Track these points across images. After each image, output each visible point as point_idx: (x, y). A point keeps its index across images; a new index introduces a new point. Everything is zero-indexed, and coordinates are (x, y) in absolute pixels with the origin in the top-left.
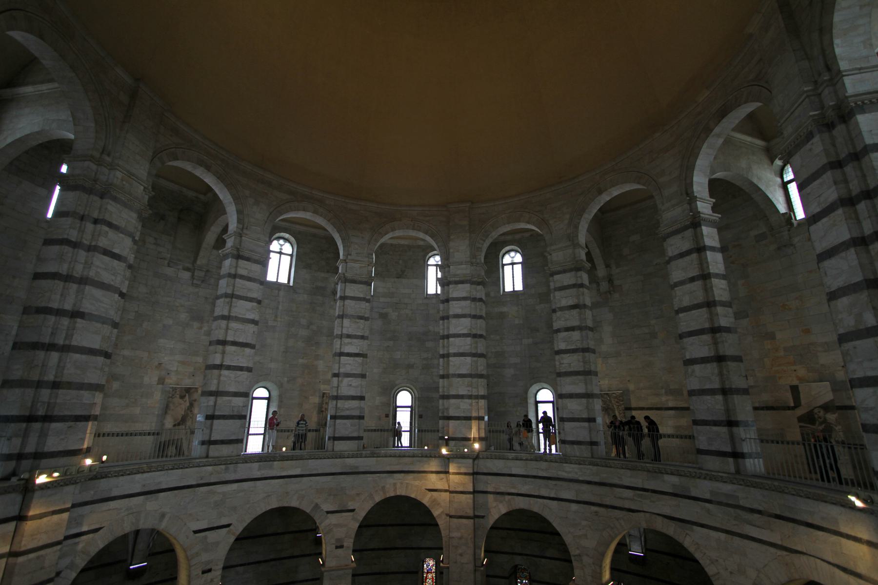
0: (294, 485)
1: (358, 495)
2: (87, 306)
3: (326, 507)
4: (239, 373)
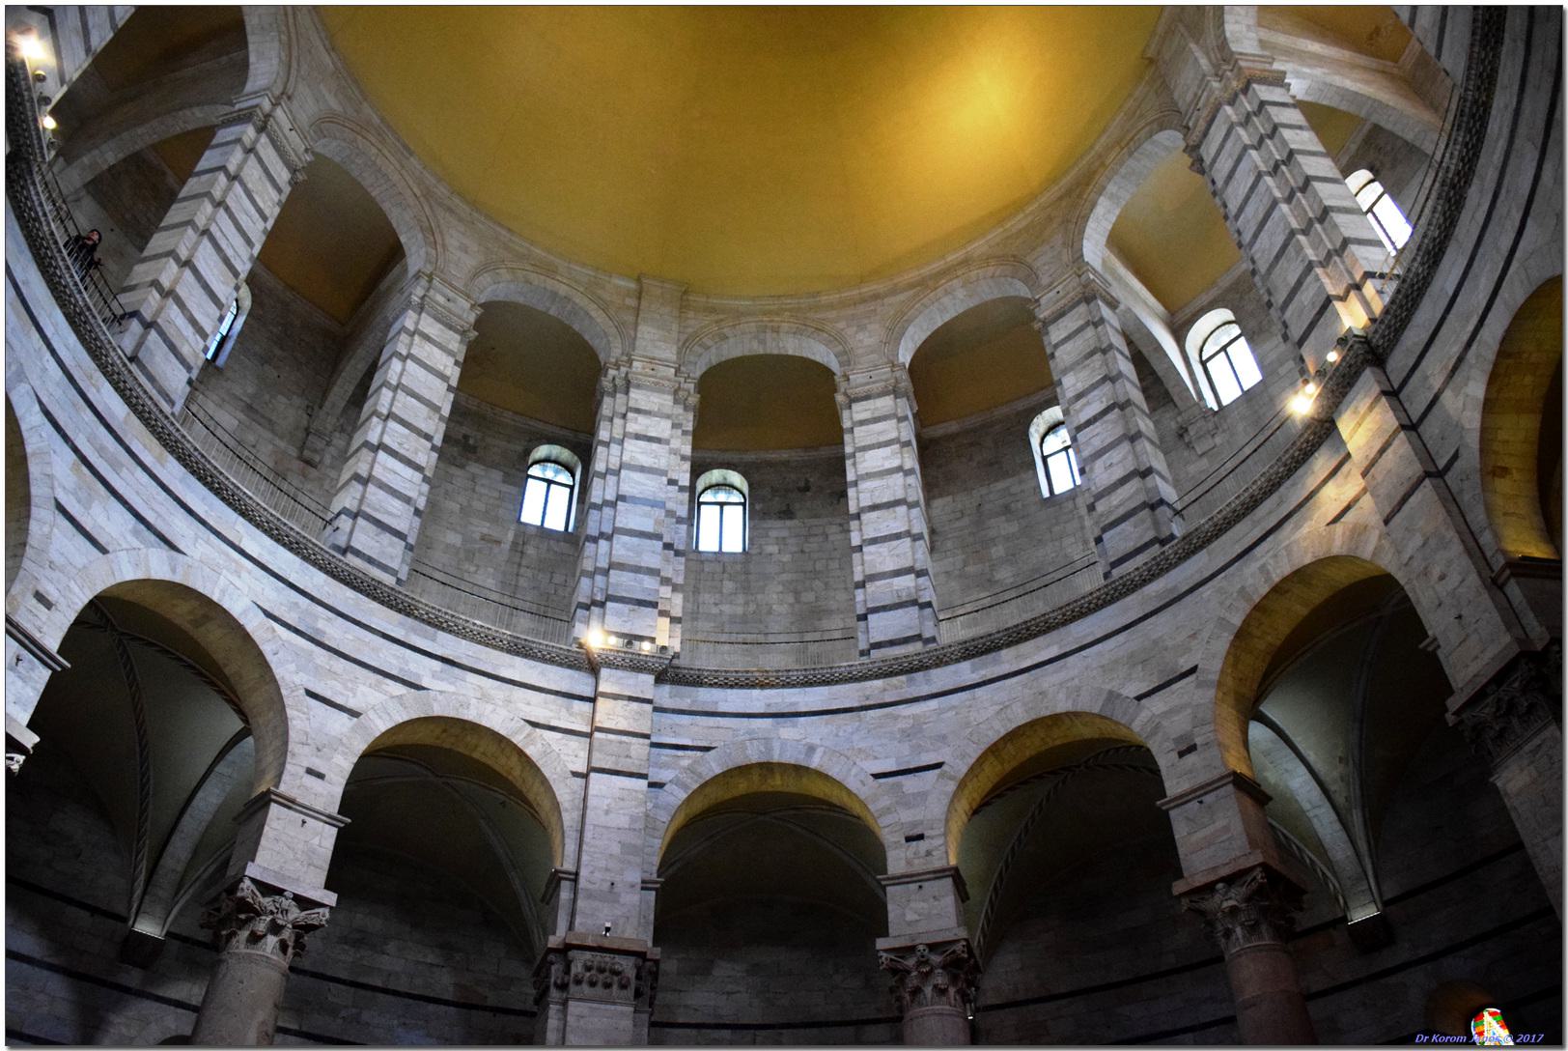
0: (1049, 678)
1: (1194, 636)
2: (626, 489)
3: (1133, 689)
4: (895, 543)
